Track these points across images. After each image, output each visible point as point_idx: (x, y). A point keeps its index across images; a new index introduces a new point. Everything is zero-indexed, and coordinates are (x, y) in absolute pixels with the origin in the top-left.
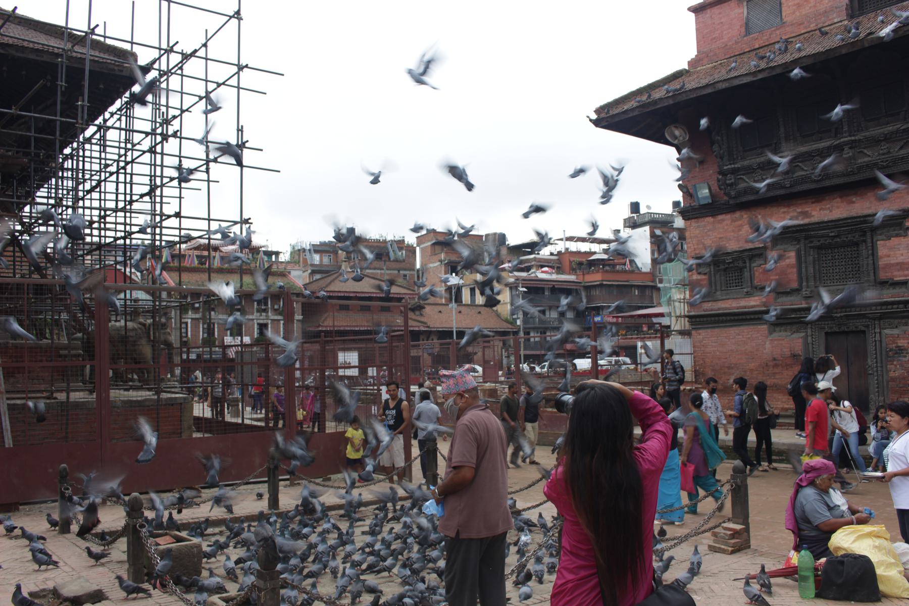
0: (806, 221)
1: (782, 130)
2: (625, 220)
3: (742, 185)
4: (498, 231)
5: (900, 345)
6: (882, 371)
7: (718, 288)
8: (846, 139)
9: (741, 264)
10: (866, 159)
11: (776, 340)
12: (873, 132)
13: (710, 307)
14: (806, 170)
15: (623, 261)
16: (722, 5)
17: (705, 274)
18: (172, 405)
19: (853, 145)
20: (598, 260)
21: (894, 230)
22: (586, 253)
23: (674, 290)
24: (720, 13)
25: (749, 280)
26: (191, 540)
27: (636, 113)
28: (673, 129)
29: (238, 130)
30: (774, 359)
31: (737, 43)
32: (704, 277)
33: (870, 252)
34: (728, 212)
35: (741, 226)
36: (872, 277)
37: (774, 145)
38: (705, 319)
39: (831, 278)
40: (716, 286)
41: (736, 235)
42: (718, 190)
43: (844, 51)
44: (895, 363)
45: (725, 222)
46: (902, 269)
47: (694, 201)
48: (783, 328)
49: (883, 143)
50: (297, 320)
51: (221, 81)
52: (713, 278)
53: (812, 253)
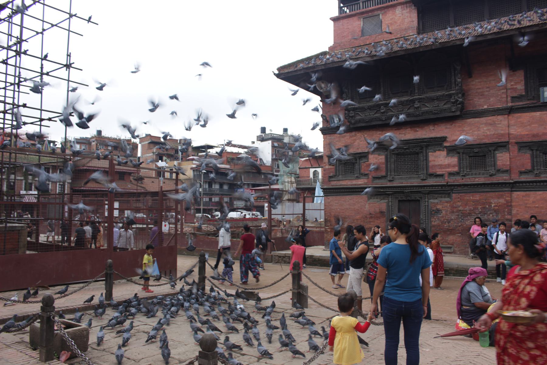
1: (382, 89)
3: (358, 118)
6: (428, 222)
7: (341, 173)
8: (417, 97)
10: (427, 109)
11: (372, 203)
13: (335, 184)
15: (256, 159)
18: (13, 231)
19: (420, 100)
22: (236, 153)
23: (285, 176)
24: (348, 23)
25: (358, 170)
26: (80, 326)
27: (302, 72)
28: (321, 83)
29: (68, 55)
30: (370, 214)
32: (332, 167)
34: (349, 132)
35: (355, 140)
36: (425, 172)
38: (332, 190)
43: (421, 50)
44: (435, 217)
45: (346, 137)
46: (441, 168)
48: (375, 197)
50: (68, 183)
51: (54, 24)
52: (338, 168)
53: (393, 157)
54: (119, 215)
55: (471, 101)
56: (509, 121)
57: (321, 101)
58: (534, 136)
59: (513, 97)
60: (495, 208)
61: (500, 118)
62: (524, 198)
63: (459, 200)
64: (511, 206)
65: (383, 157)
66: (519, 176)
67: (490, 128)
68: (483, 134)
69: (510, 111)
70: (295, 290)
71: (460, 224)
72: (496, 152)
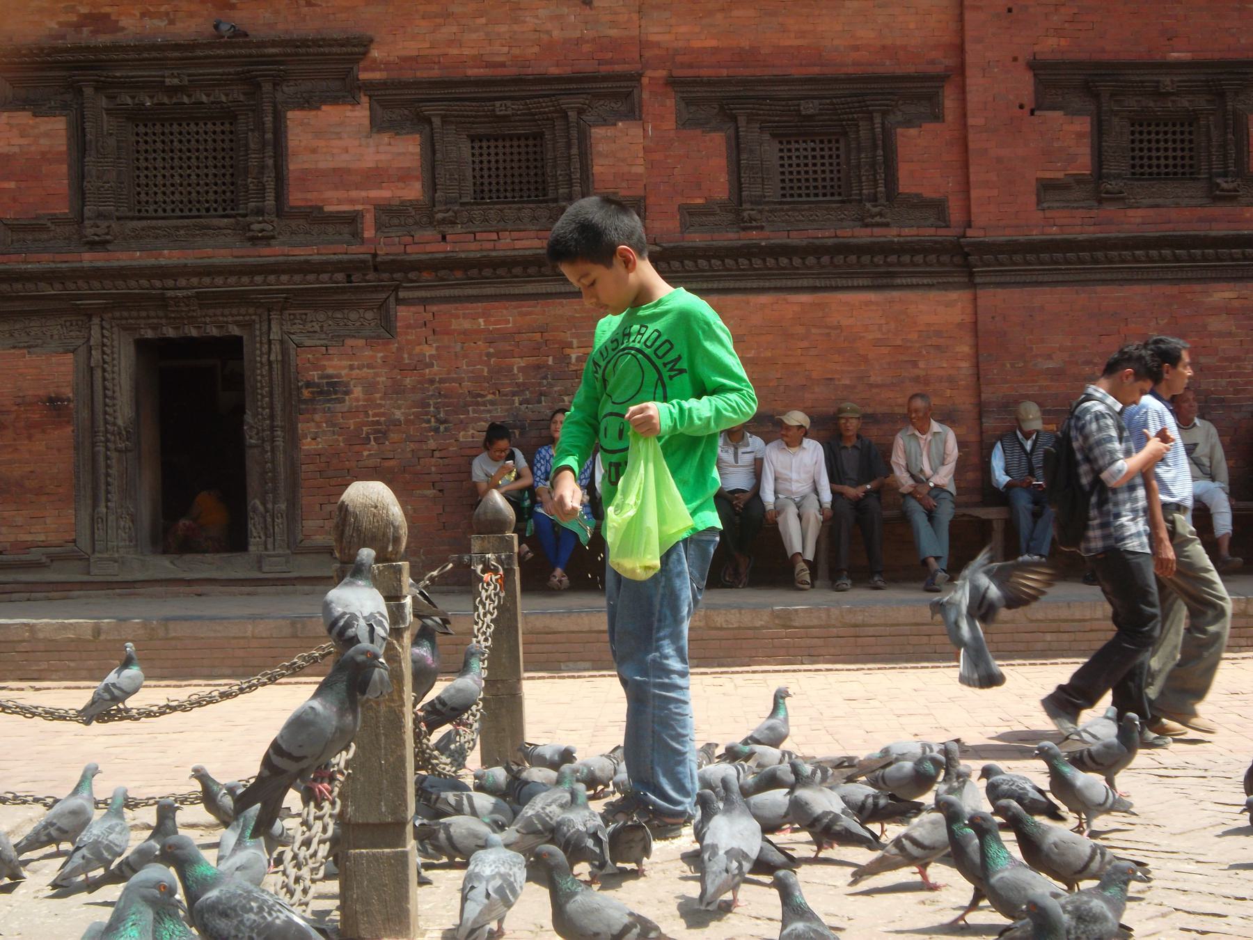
0: (104, 39)
5: (330, 371)
39: (160, 198)
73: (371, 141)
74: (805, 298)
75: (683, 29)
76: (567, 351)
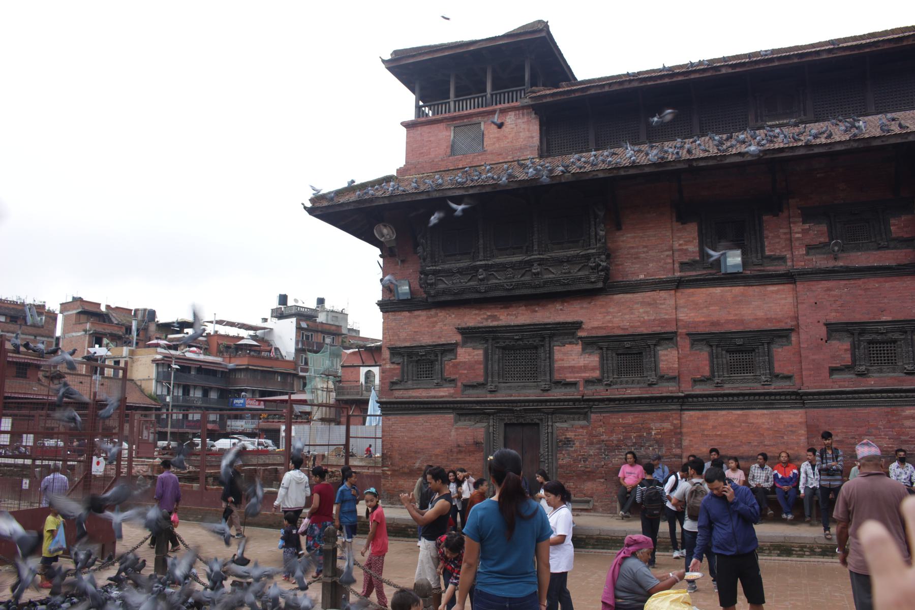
0: (495, 323)
1: (481, 242)
2: (272, 310)
3: (441, 286)
4: (149, 307)
5: (568, 437)
6: (552, 459)
7: (410, 377)
8: (536, 257)
9: (433, 358)
10: (551, 276)
12: (558, 254)
13: (400, 395)
14: (500, 279)
15: (269, 348)
16: (432, 126)
17: (398, 364)
19: (541, 262)
20: (246, 345)
21: (568, 338)
22: (233, 337)
23: (318, 379)
24: (430, 132)
25: (440, 372)
27: (351, 207)
28: (382, 227)
30: (459, 446)
31: (442, 160)
32: (396, 366)
33: (548, 355)
34: (426, 309)
35: (436, 322)
36: (548, 378)
37: (472, 254)
38: (396, 406)
39: (513, 375)
40: (408, 376)
41: (430, 331)
42: (419, 288)
44: (563, 452)
45: (421, 318)
46: (572, 372)
47: (394, 296)
48: (467, 418)
49: (565, 264)
52: (406, 369)
54: (11, 441)
55: (620, 267)
56: (677, 300)
57: (381, 256)
58: (713, 324)
59: (682, 264)
60: (657, 436)
61: (663, 294)
62: (700, 421)
63: (601, 423)
64: (681, 433)
65: (481, 352)
66: (693, 386)
67: (649, 310)
68: (638, 319)
69: (679, 284)
70: (327, 578)
71: (603, 463)
72: (658, 348)
73: (582, 357)
74: (739, 412)
75: (692, 314)
76: (651, 431)
